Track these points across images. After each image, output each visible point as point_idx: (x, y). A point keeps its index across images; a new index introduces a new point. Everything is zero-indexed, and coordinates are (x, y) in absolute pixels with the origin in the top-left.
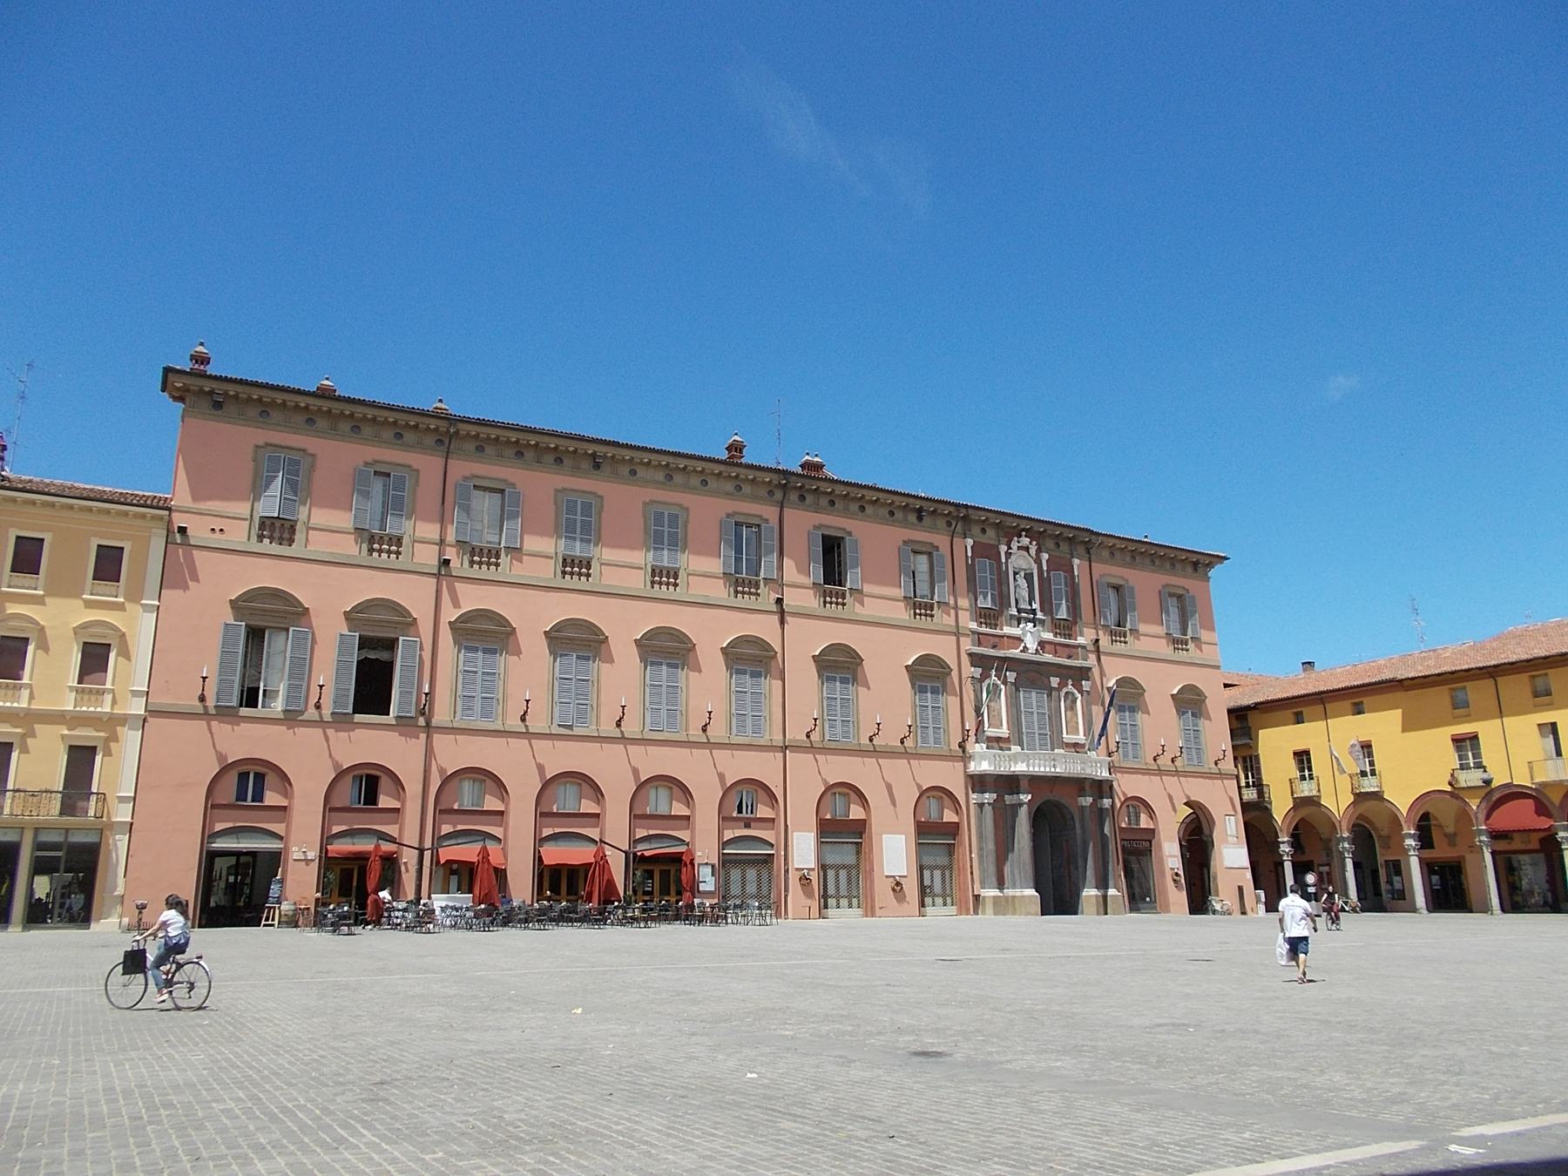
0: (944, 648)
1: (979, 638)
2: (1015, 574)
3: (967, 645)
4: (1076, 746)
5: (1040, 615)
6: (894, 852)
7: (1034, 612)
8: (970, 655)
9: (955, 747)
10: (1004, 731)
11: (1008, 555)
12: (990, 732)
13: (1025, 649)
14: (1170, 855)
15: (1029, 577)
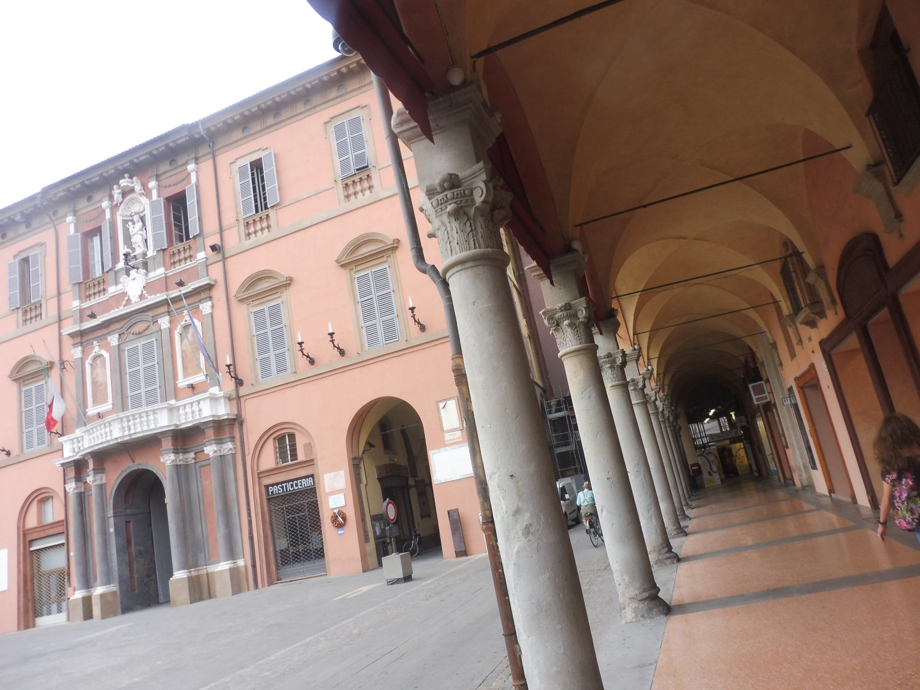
0: (42, 344)
1: (83, 315)
2: (125, 222)
3: (70, 327)
7: (145, 254)
8: (72, 335)
10: (108, 406)
11: (114, 208)
12: (92, 411)
13: (129, 302)
14: (336, 490)
15: (143, 219)
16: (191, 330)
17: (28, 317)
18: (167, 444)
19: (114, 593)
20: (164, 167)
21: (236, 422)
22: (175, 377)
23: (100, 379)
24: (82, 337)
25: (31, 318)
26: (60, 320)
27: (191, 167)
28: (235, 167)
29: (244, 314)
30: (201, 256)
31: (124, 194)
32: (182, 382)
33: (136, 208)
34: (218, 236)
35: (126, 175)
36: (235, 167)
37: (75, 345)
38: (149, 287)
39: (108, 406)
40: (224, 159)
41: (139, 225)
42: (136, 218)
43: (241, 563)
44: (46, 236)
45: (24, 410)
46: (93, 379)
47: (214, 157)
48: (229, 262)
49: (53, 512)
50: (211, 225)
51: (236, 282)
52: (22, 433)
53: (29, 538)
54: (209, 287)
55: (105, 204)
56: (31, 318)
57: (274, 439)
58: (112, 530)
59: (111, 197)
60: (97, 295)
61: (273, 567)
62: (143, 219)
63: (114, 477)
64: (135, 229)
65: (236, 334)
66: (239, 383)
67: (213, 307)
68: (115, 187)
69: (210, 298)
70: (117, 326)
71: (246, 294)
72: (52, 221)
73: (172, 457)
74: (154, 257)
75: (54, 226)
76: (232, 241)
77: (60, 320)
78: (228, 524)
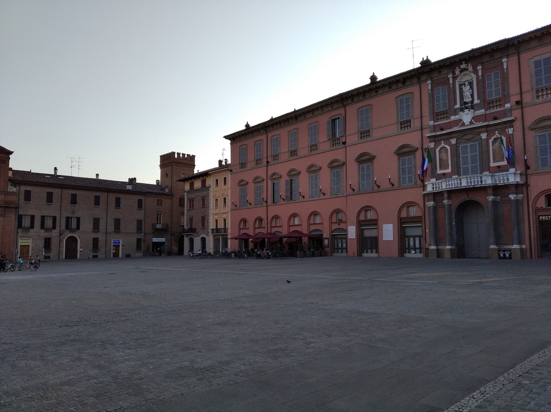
0: (412, 139)
1: (435, 128)
2: (460, 85)
4: (499, 169)
5: (476, 101)
6: (388, 232)
7: (472, 102)
8: (429, 137)
9: (419, 182)
10: (449, 170)
11: (455, 78)
12: (439, 172)
13: (463, 124)
15: (471, 84)
16: (499, 141)
17: (403, 126)
18: (490, 191)
19: (454, 249)
20: (486, 59)
21: (526, 185)
22: (489, 162)
23: (444, 158)
24: (433, 138)
25: (404, 127)
26: (422, 129)
27: (504, 60)
28: (532, 61)
29: (531, 136)
30: (508, 106)
31: (461, 72)
32: (492, 164)
33: (467, 78)
34: (519, 96)
35: (464, 62)
36: (532, 61)
37: (430, 142)
38: (476, 118)
39: (449, 170)
40: (525, 56)
41: (468, 87)
42: (467, 83)
43: (524, 246)
44: (415, 89)
45: (401, 167)
46: (440, 157)
47: (519, 55)
48: (525, 109)
49: (414, 212)
50: (514, 89)
51: (529, 120)
52: (400, 177)
53: (402, 221)
54: (513, 121)
55: (450, 76)
56: (404, 127)
57: (546, 196)
58: (454, 224)
59: (454, 73)
60: (443, 120)
61: (540, 251)
62: (471, 84)
63: (457, 201)
64: (466, 89)
65: (527, 146)
66: (527, 167)
67: (513, 131)
68: (457, 68)
69: (512, 126)
70: (456, 135)
71: (536, 126)
72: (419, 82)
73: (493, 197)
74: (477, 104)
75: (420, 84)
76: (527, 98)
77: (422, 129)
78: (519, 230)
